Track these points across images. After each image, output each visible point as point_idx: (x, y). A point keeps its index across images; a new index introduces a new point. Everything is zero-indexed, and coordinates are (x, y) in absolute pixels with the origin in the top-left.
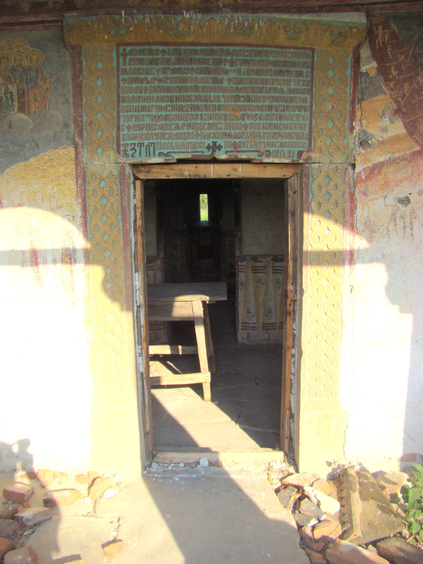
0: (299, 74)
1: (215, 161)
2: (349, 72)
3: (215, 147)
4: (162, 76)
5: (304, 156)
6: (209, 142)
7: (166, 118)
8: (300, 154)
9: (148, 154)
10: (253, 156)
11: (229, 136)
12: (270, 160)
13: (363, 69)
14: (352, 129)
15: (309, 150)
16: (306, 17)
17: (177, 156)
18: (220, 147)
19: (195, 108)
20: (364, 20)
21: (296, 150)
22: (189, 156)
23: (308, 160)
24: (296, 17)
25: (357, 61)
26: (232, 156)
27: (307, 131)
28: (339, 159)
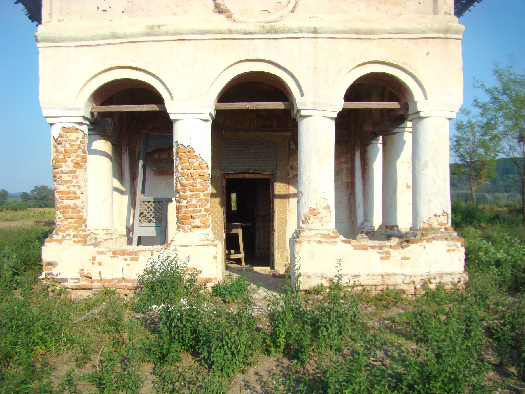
0: (273, 149)
1: (248, 173)
2: (287, 148)
3: (249, 169)
4: (234, 148)
5: (275, 172)
6: (247, 167)
7: (235, 161)
8: (273, 171)
9: (229, 171)
10: (259, 172)
11: (253, 166)
12: (265, 173)
13: (291, 147)
14: (288, 164)
15: (276, 170)
16: (275, 133)
17: (238, 172)
18: (250, 169)
19: (243, 158)
20: (291, 134)
21: (272, 170)
22: (241, 171)
23: (276, 173)
24: (272, 133)
25: (290, 145)
26: (254, 172)
27: (275, 165)
28: (285, 173)
